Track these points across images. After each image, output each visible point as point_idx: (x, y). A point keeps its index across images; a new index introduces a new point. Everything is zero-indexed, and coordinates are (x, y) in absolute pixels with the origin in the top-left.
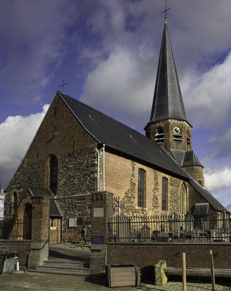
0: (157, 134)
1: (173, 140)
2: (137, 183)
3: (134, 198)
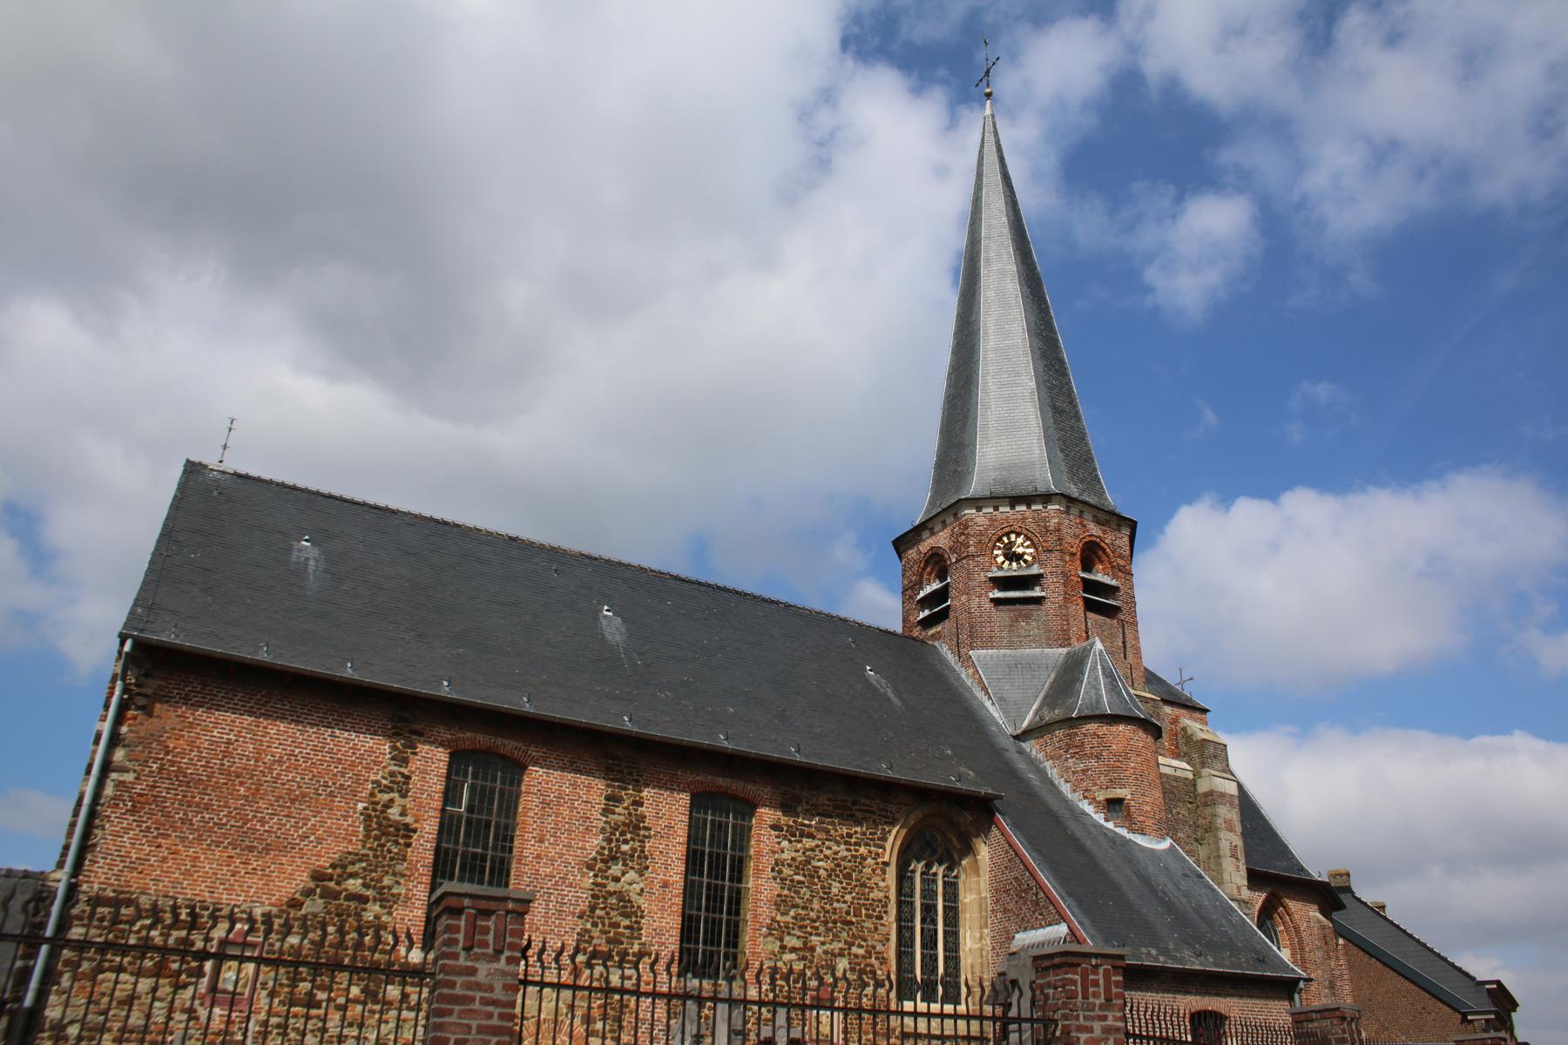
0: (936, 585)
1: (988, 605)
2: (429, 828)
3: (387, 899)
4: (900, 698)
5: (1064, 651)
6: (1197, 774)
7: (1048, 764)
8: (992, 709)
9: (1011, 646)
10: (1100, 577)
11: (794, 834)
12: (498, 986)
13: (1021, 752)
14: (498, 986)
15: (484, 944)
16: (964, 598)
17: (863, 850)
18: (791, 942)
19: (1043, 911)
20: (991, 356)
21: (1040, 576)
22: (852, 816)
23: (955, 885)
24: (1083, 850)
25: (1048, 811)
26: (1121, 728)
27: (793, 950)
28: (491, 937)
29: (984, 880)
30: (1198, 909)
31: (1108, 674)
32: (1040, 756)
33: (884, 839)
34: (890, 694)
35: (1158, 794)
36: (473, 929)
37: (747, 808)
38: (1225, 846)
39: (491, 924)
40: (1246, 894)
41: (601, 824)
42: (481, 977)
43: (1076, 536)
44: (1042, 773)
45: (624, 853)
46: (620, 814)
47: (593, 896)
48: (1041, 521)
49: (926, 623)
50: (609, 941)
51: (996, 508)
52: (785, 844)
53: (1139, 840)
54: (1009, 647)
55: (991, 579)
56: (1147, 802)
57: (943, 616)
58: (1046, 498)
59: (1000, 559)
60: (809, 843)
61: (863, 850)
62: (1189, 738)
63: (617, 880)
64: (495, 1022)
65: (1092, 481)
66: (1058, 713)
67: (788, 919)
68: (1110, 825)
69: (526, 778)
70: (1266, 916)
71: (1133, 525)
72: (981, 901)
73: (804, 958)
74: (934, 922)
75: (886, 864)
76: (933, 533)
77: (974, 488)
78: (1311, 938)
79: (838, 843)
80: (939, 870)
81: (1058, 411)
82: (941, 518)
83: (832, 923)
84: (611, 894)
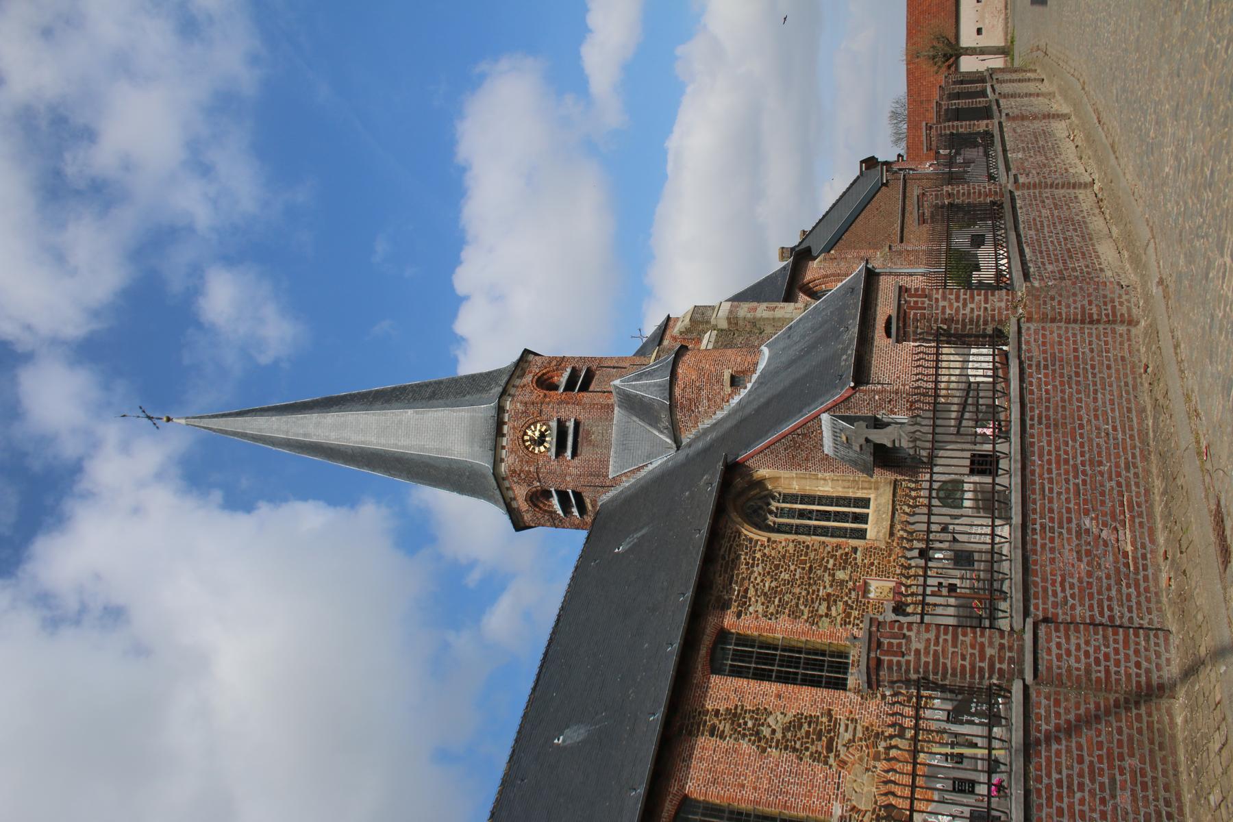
0: (555, 501)
1: (576, 461)
4: (642, 528)
5: (616, 409)
6: (714, 328)
7: (701, 426)
8: (655, 465)
9: (608, 447)
10: (563, 379)
11: (744, 601)
12: (926, 636)
13: (689, 445)
14: (926, 636)
15: (899, 645)
16: (568, 479)
17: (758, 555)
18: (823, 609)
19: (810, 431)
20: (383, 441)
21: (559, 420)
22: (733, 561)
23: (785, 495)
24: (768, 403)
25: (738, 426)
26: (680, 371)
27: (829, 608)
28: (895, 641)
29: (783, 473)
30: (814, 330)
31: (639, 377)
32: (694, 431)
33: (751, 540)
34: (639, 535)
35: (729, 352)
36: (887, 653)
37: (723, 635)
38: (766, 314)
39: (886, 641)
40: (800, 305)
41: (732, 741)
42: (921, 646)
43: (532, 392)
44: (706, 432)
45: (754, 725)
46: (725, 726)
47: (786, 749)
48: (517, 416)
49: (582, 509)
50: (819, 739)
51: (503, 447)
52: (751, 609)
53: (761, 367)
54: (609, 449)
55: (557, 456)
56: (734, 359)
57: (578, 495)
58: (501, 409)
59: (542, 449)
60: (751, 592)
61: (758, 555)
62: (688, 331)
63: (774, 731)
64: (949, 637)
65: (490, 377)
66: (664, 416)
67: (806, 611)
68: (749, 386)
69: (694, 796)
70: (814, 295)
71: (527, 352)
72: (799, 478)
73: (835, 601)
74: (811, 512)
75: (769, 540)
76: (515, 499)
77: (487, 465)
78: (831, 268)
79: (752, 572)
80: (774, 505)
81: (433, 396)
82: (505, 491)
83: (810, 580)
84: (784, 737)
